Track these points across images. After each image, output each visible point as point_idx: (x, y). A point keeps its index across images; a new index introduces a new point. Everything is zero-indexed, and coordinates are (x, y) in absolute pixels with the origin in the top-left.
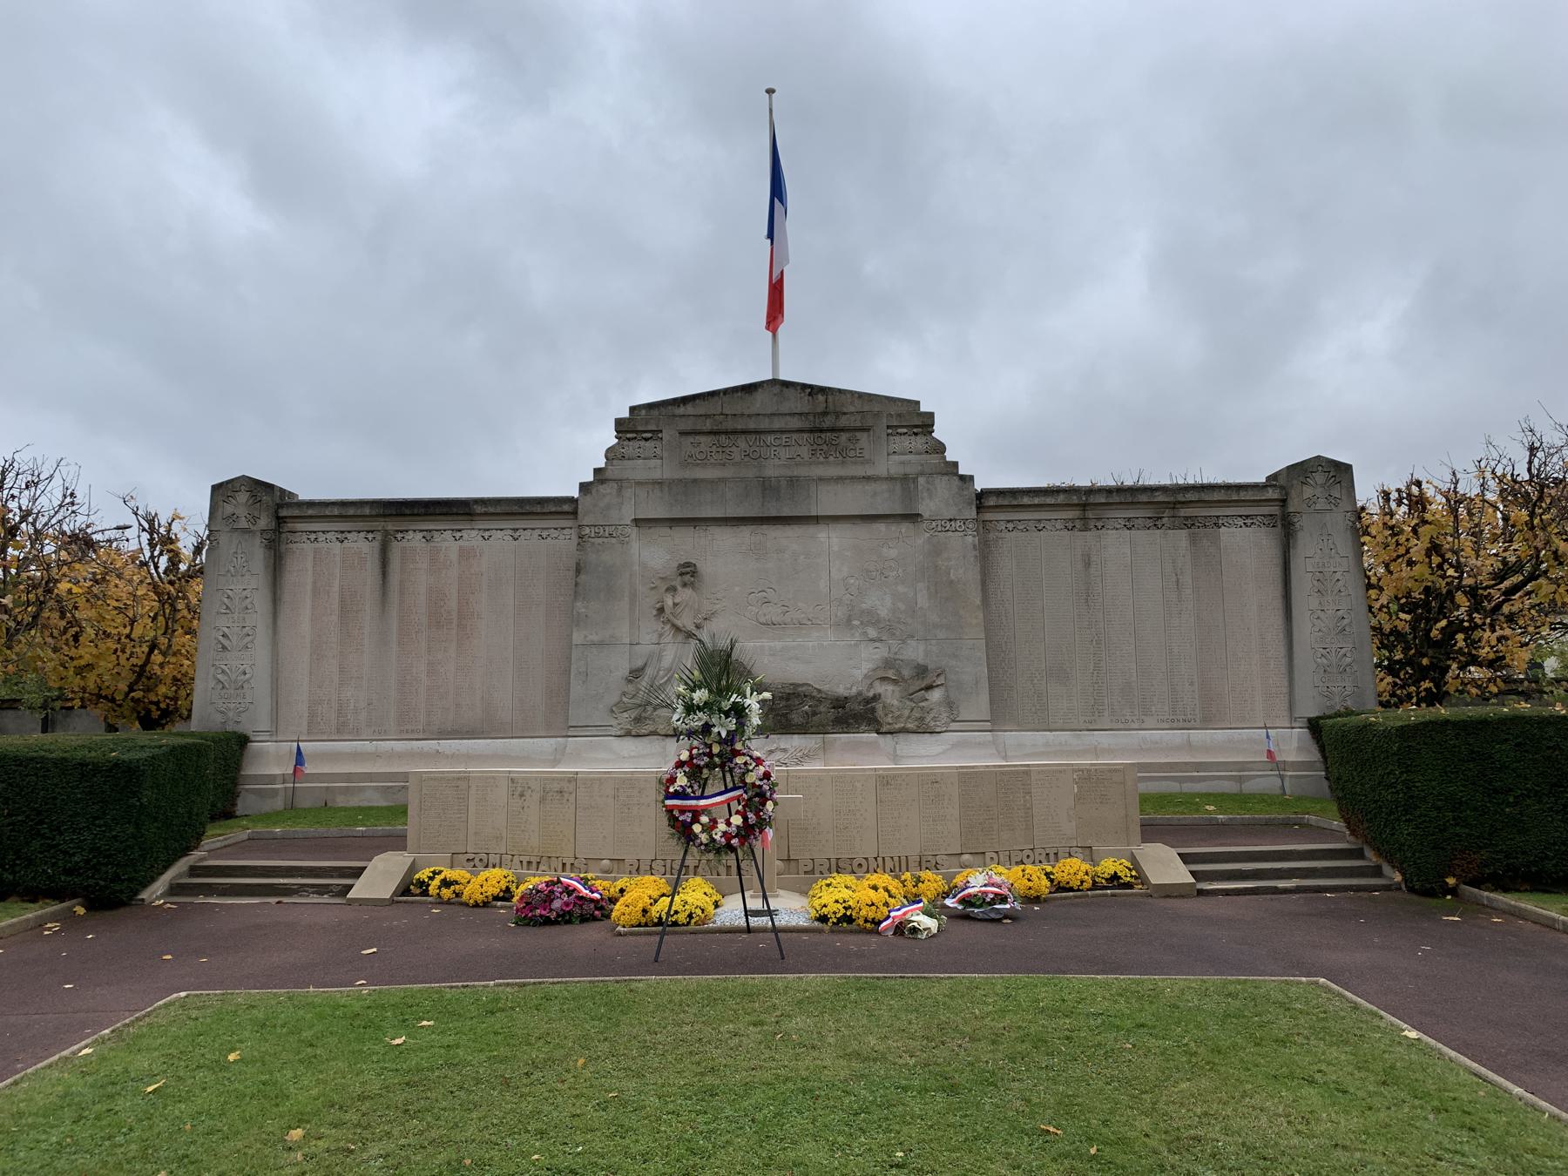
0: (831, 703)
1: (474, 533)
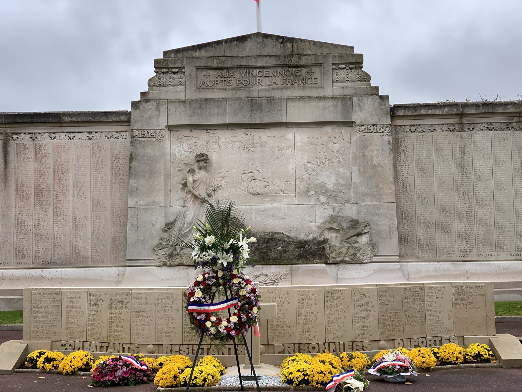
1: (63, 135)
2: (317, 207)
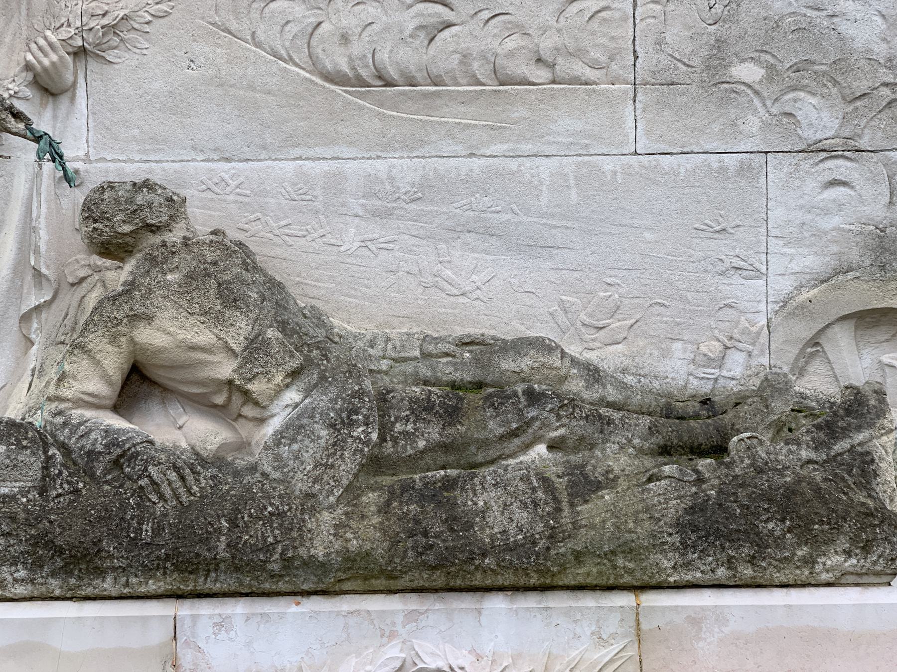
0: (652, 430)
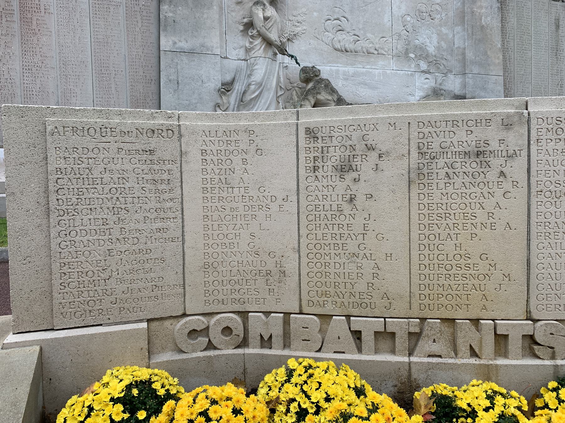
2: (417, 75)
